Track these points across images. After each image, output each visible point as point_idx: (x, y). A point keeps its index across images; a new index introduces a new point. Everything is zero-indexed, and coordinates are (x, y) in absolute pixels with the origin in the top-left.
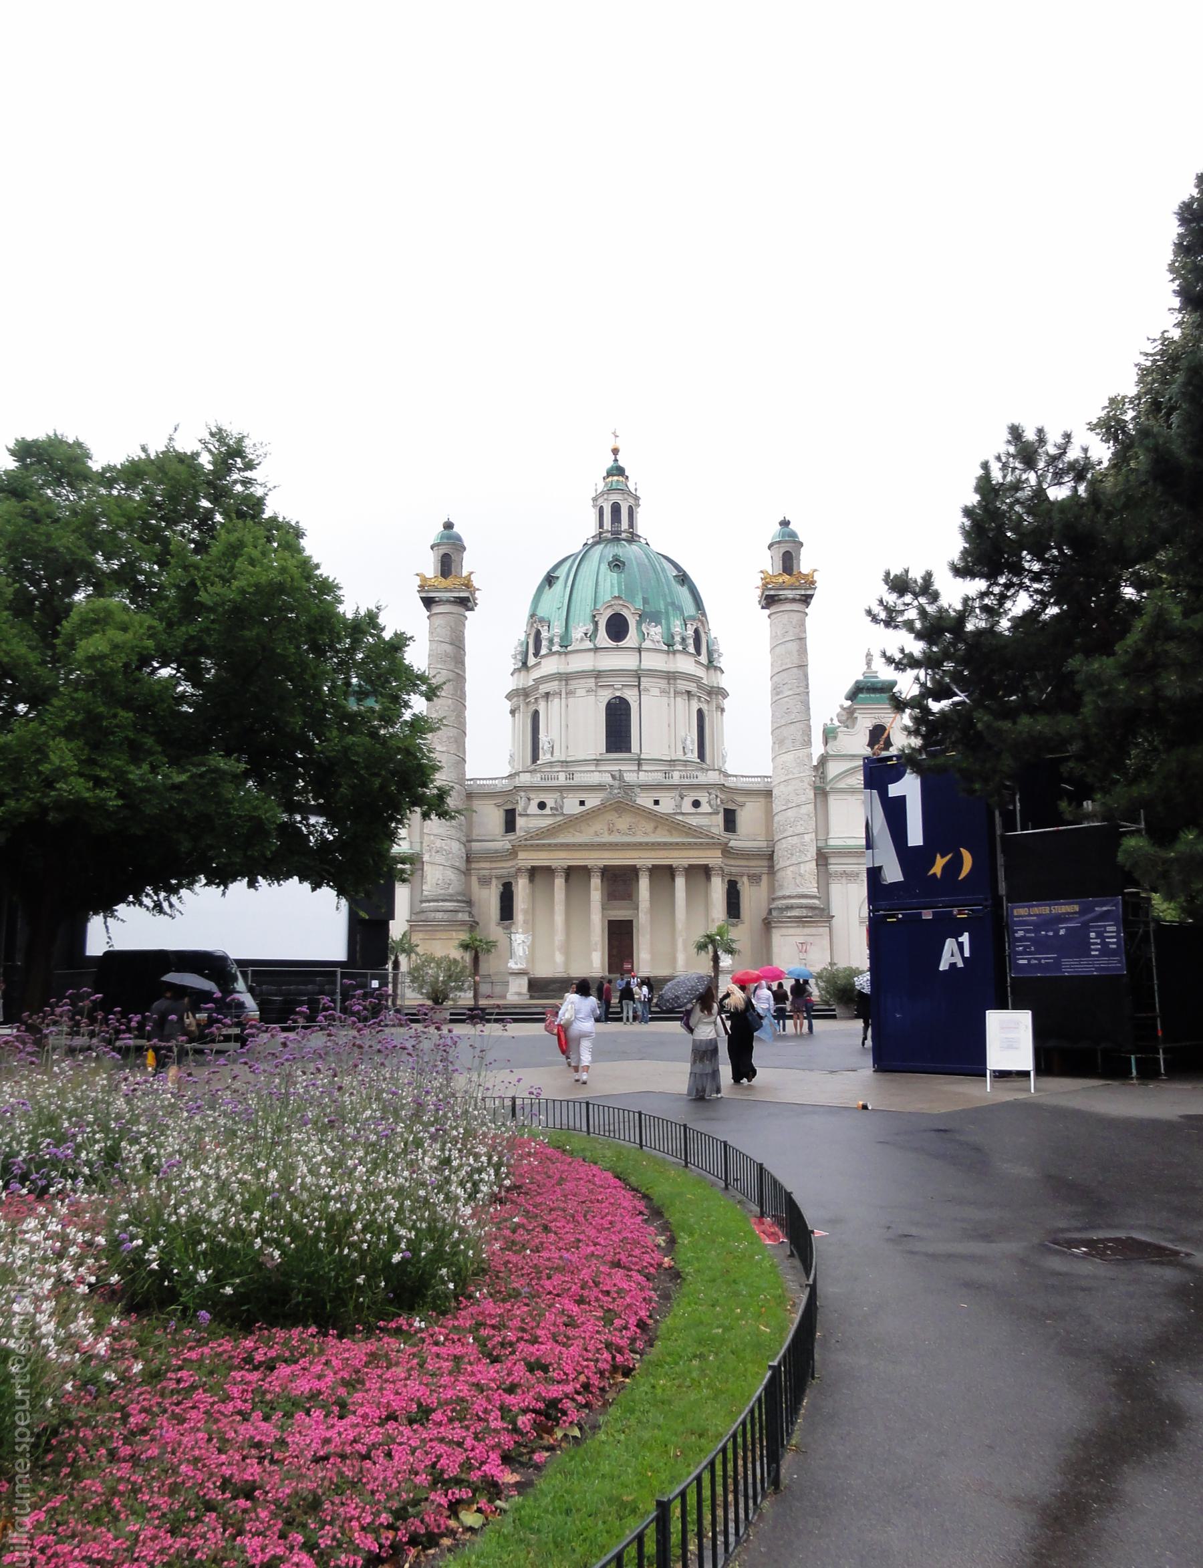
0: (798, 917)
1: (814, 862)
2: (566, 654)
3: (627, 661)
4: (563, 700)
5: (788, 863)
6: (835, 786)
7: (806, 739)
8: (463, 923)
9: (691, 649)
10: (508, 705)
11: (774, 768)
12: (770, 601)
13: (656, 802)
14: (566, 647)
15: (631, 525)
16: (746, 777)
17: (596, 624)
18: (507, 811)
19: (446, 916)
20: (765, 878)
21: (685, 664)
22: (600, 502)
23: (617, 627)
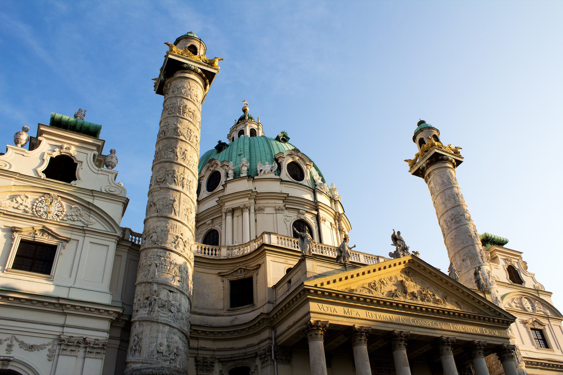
18: (232, 283)
22: (240, 128)
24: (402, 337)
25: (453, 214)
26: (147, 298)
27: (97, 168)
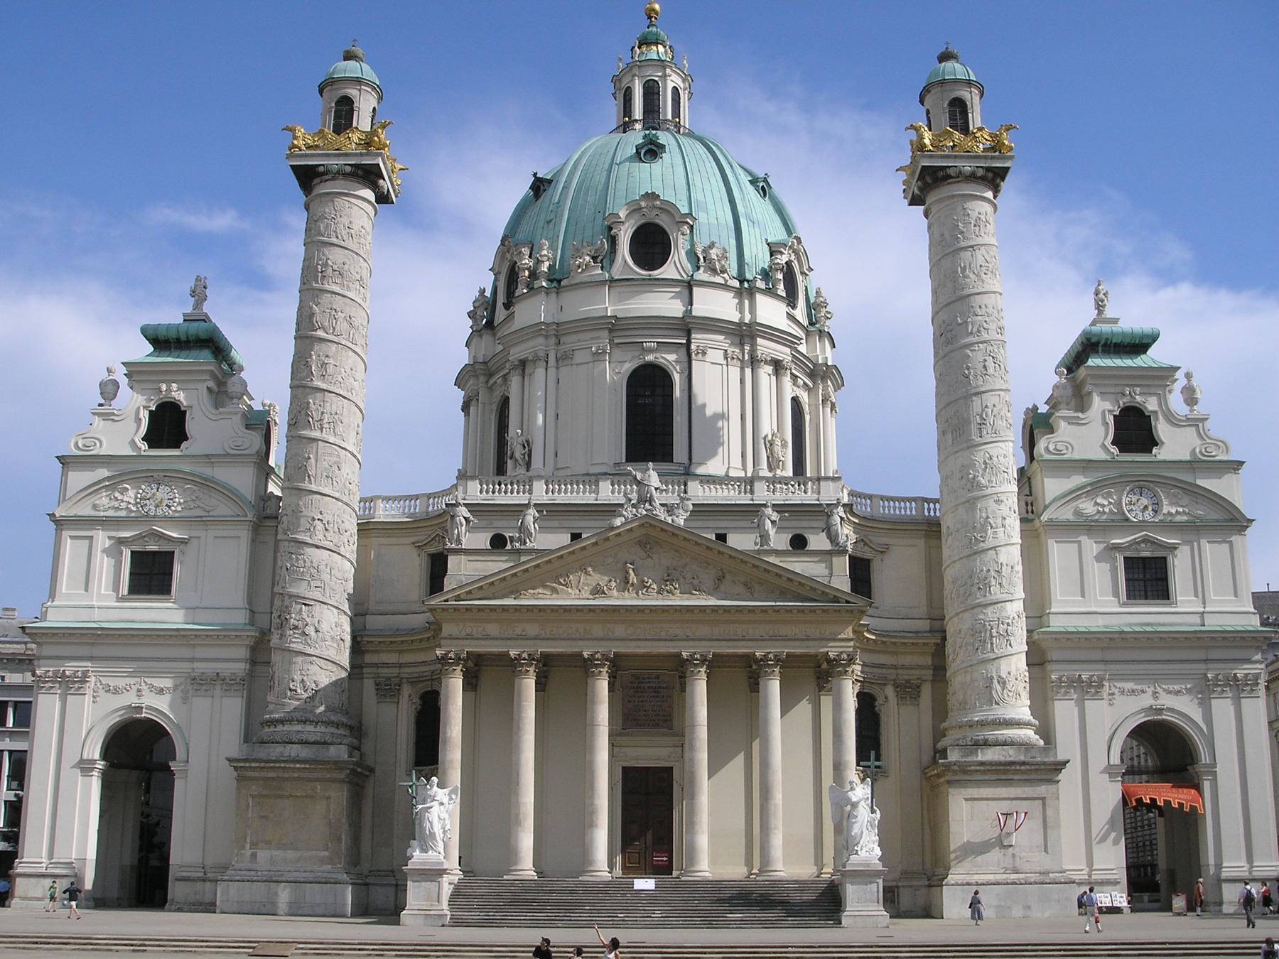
0: (1000, 764)
1: (1024, 656)
3: (667, 305)
4: (552, 371)
6: (1053, 516)
8: (337, 765)
9: (781, 291)
10: (459, 395)
11: (945, 479)
13: (722, 538)
14: (559, 282)
15: (676, 112)
16: (889, 499)
17: (613, 241)
19: (304, 752)
20: (926, 690)
21: (771, 311)
22: (624, 84)
24: (598, 660)
25: (944, 321)
26: (279, 616)
27: (214, 411)
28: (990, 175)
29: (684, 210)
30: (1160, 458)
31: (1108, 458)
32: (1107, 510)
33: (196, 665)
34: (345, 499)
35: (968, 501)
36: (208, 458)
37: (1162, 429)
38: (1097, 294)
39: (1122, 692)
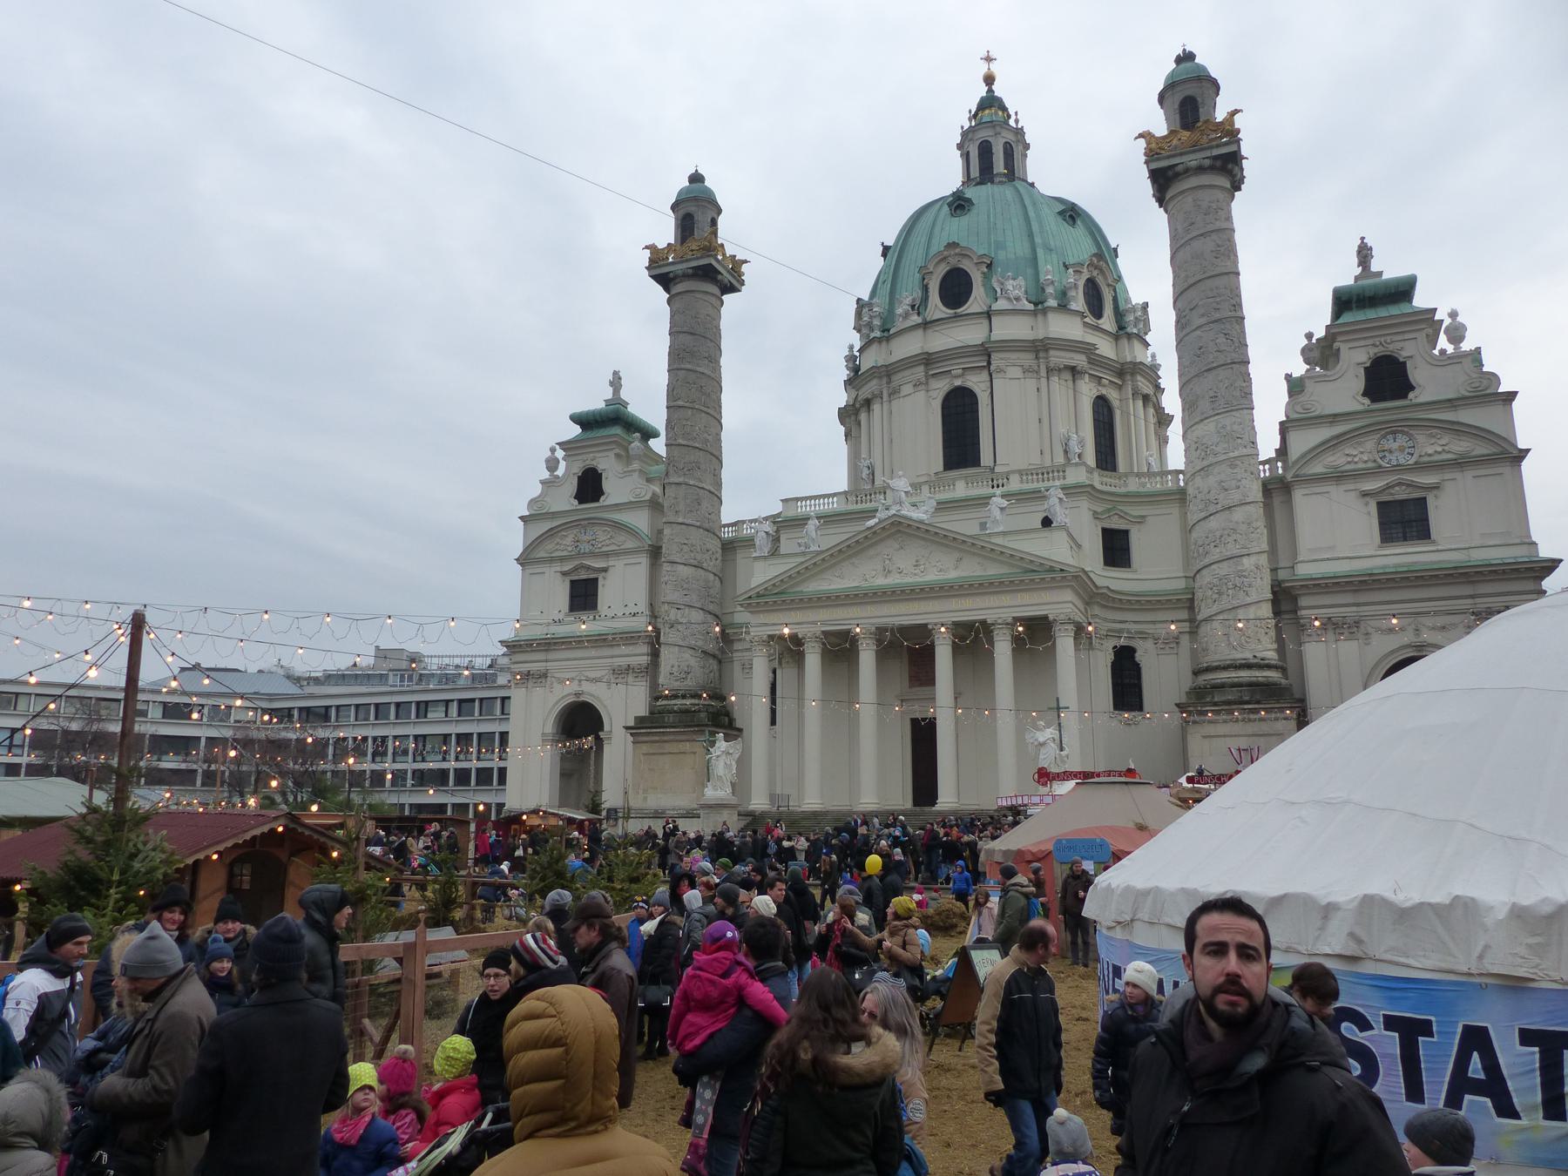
2: (888, 339)
3: (969, 334)
5: (1215, 609)
7: (1238, 393)
12: (1164, 180)
13: (983, 526)
14: (889, 331)
17: (925, 289)
23: (956, 289)
28: (1218, 163)
29: (981, 252)
30: (1421, 400)
31: (1360, 408)
32: (1356, 460)
33: (615, 660)
34: (706, 525)
35: (1202, 469)
36: (618, 507)
37: (1416, 374)
38: (1359, 252)
39: (1378, 629)
